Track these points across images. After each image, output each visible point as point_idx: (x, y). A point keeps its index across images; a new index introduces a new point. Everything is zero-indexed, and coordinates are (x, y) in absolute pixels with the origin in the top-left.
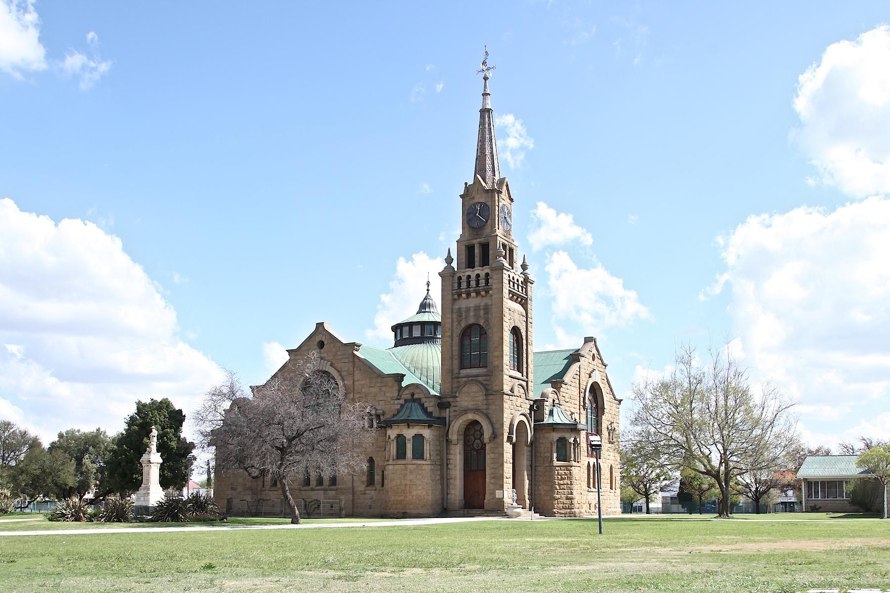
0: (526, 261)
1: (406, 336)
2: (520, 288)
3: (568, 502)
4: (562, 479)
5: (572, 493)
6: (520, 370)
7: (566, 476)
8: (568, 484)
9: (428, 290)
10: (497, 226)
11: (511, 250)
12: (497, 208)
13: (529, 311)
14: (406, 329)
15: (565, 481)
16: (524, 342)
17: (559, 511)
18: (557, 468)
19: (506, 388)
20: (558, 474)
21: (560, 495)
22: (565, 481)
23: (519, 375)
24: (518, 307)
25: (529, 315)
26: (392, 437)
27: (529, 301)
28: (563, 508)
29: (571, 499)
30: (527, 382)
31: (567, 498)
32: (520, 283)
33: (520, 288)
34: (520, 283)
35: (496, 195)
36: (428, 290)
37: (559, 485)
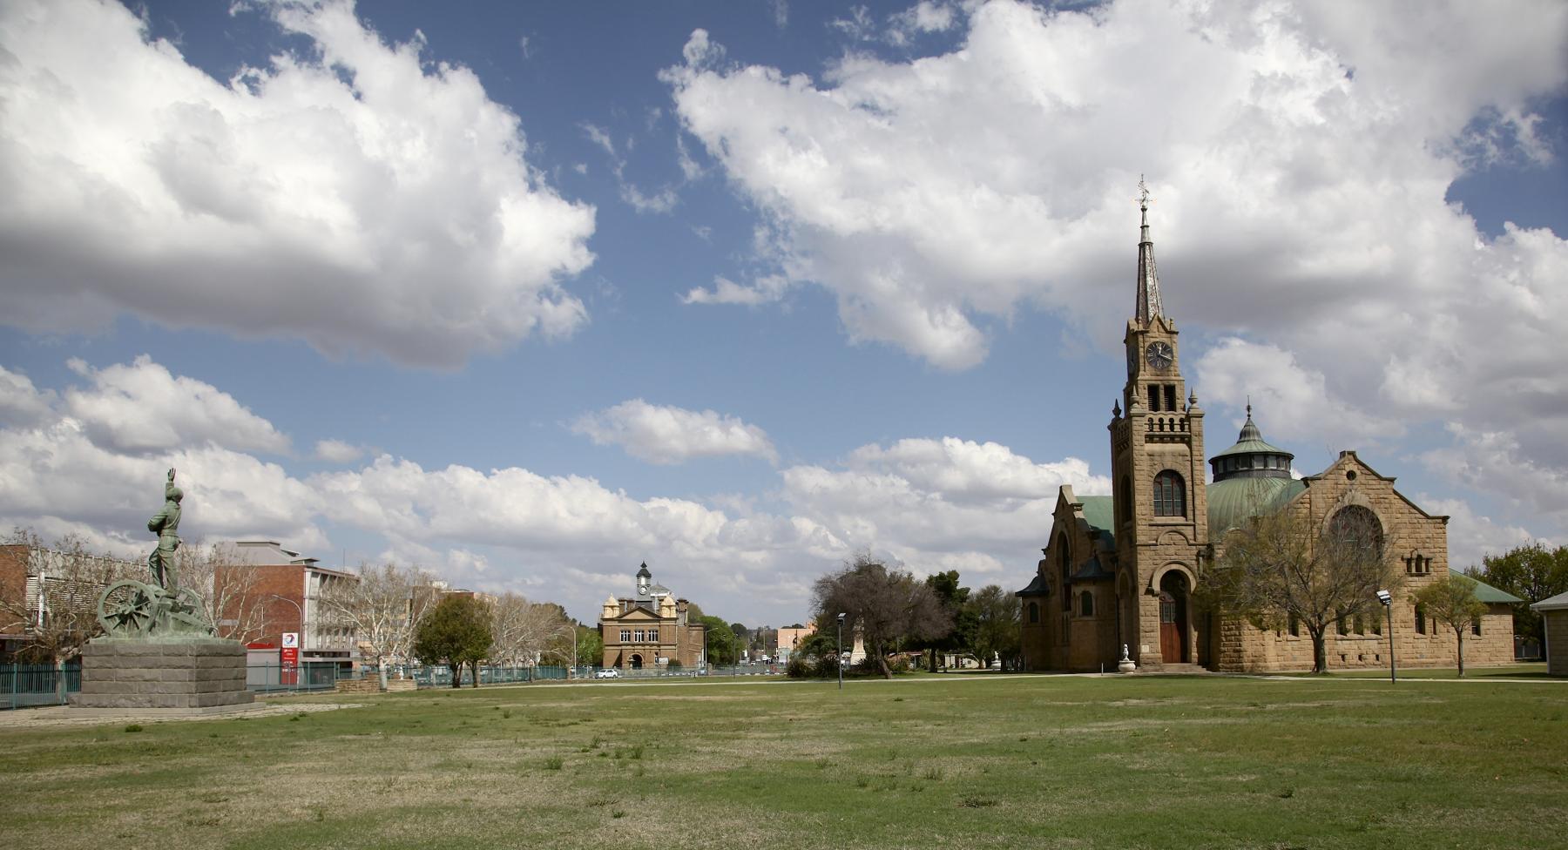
0: (1194, 394)
1: (1221, 471)
2: (1177, 428)
3: (1236, 654)
4: (1229, 630)
5: (1240, 645)
6: (1184, 514)
7: (1234, 627)
8: (1235, 635)
9: (1249, 416)
10: (1142, 368)
11: (1170, 391)
12: (1141, 350)
13: (1194, 447)
14: (1221, 464)
15: (1232, 632)
16: (1188, 484)
17: (1225, 665)
18: (1223, 618)
19: (1141, 539)
20: (1224, 625)
21: (1226, 648)
22: (1232, 632)
23: (1181, 520)
24: (1183, 447)
25: (1194, 453)
26: (1077, 594)
27: (1194, 437)
28: (1230, 662)
29: (1239, 651)
30: (1194, 526)
31: (1235, 651)
32: (1177, 421)
33: (1177, 428)
34: (1177, 421)
35: (1141, 339)
36: (1249, 416)
37: (1226, 636)
